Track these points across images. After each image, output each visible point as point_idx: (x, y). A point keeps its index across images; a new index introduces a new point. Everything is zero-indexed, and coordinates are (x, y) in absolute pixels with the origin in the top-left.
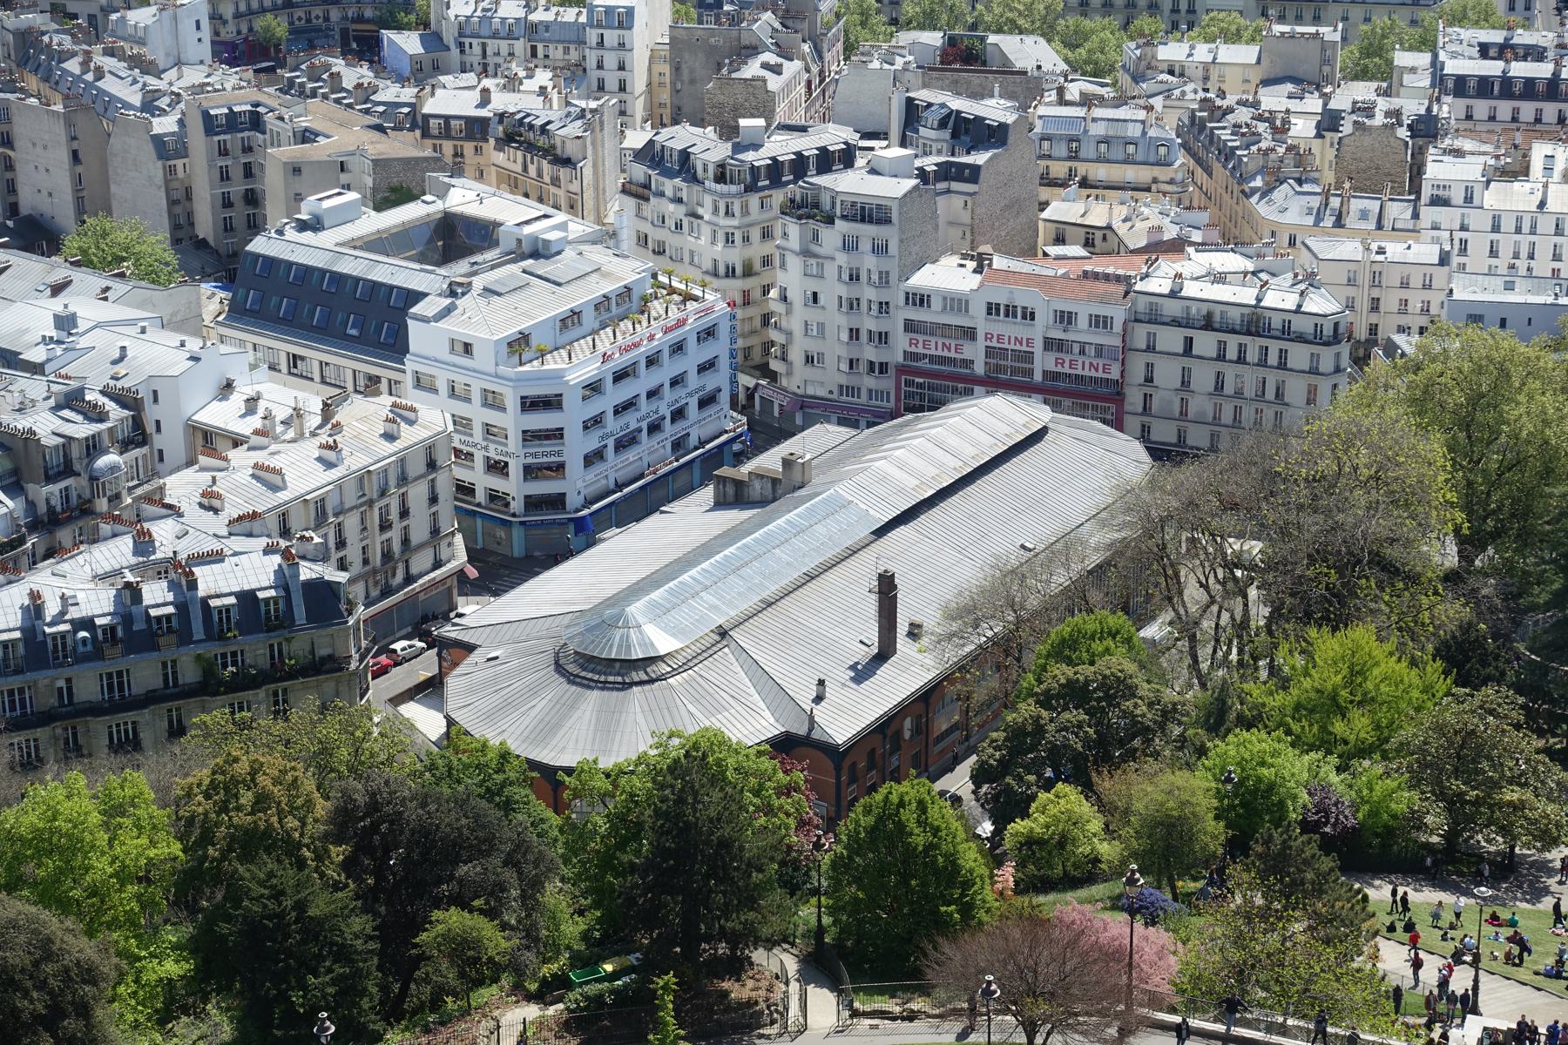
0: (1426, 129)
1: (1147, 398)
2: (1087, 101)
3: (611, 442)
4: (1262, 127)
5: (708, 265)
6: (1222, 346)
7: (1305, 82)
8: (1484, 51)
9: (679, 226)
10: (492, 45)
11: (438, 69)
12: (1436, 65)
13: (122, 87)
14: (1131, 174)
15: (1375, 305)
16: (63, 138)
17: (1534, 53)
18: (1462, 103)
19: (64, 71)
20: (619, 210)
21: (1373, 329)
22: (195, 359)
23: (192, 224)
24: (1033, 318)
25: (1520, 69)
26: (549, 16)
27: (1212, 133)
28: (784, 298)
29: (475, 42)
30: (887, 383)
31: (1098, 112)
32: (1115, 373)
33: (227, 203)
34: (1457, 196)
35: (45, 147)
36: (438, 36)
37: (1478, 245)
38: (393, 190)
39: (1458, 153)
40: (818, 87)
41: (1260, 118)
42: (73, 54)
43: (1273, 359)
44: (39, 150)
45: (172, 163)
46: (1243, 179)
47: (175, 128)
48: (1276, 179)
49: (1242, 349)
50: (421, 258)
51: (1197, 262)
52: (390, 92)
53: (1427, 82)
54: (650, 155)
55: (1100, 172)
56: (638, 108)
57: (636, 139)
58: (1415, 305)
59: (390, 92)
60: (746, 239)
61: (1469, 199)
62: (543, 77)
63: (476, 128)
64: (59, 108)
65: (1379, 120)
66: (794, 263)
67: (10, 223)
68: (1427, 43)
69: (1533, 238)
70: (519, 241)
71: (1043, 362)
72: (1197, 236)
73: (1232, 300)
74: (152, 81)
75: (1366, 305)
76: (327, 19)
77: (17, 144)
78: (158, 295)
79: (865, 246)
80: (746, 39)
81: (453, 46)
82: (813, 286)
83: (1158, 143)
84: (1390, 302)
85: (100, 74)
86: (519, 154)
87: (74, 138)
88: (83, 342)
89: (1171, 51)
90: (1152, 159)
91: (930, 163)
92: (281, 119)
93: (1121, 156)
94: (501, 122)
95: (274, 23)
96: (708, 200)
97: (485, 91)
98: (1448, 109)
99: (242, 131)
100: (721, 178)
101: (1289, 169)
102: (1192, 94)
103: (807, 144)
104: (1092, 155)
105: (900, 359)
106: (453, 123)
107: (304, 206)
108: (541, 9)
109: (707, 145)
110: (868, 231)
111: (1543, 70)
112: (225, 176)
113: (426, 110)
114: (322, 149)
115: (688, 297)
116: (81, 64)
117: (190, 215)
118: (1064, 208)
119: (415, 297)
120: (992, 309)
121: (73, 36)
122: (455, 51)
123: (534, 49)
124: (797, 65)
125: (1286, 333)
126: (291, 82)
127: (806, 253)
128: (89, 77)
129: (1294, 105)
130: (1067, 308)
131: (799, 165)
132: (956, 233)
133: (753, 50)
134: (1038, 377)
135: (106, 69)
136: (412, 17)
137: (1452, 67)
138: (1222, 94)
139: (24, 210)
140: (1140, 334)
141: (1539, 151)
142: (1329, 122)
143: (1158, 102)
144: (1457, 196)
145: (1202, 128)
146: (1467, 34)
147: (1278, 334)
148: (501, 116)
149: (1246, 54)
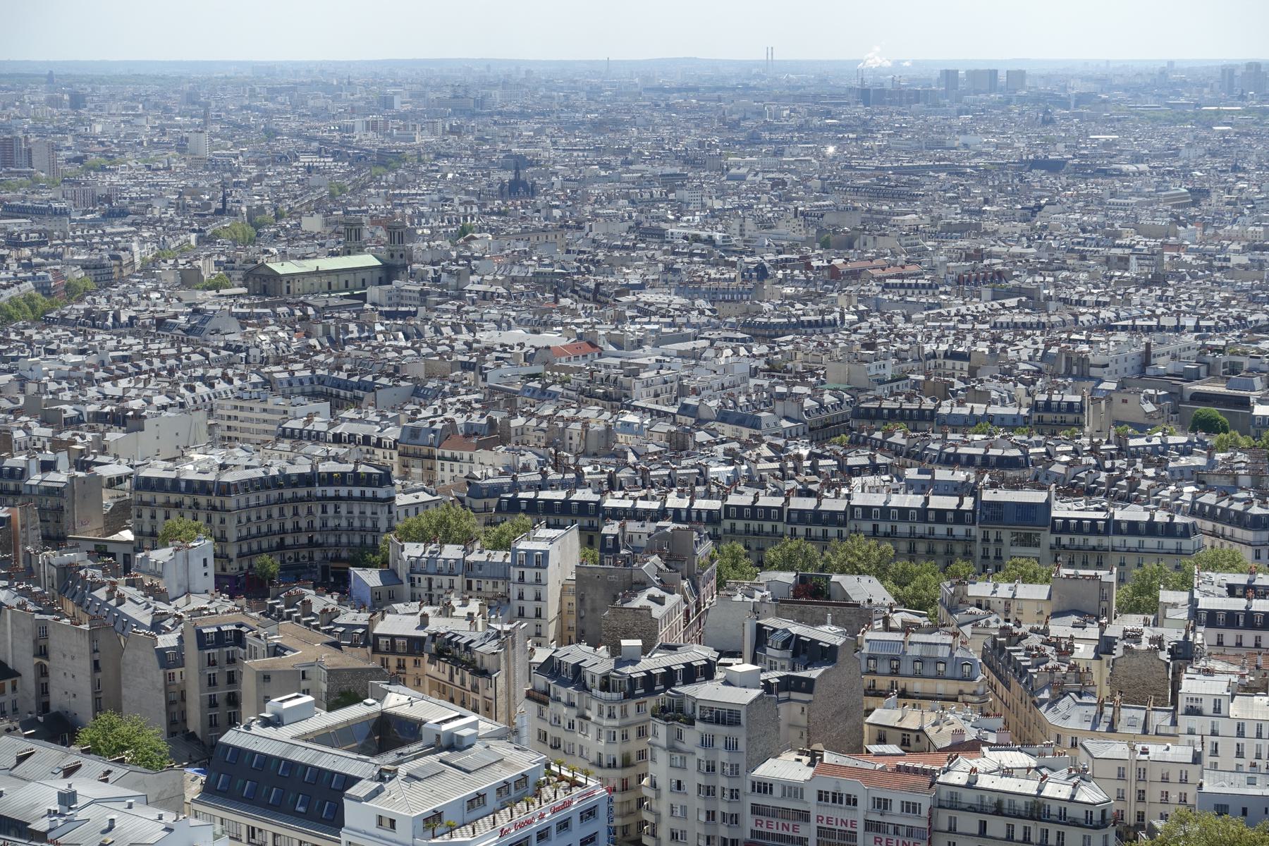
0: (1184, 653)
2: (907, 628)
4: (1049, 650)
5: (594, 758)
6: (1010, 829)
7: (1086, 615)
8: (1232, 590)
9: (571, 725)
10: (436, 580)
11: (393, 598)
12: (1193, 602)
13: (137, 610)
14: (941, 687)
15: (1141, 796)
16: (87, 651)
18: (1213, 633)
19: (94, 597)
20: (526, 712)
21: (1141, 816)
22: (169, 829)
23: (185, 721)
24: (855, 803)
26: (482, 558)
27: (1010, 655)
28: (654, 785)
29: (423, 577)
31: (914, 637)
33: (213, 703)
34: (1208, 707)
35: (73, 658)
36: (394, 573)
37: (1227, 747)
38: (343, 694)
39: (1209, 672)
40: (695, 617)
41: (1048, 643)
42: (103, 585)
44: (68, 660)
45: (171, 671)
46: (1034, 692)
47: (176, 644)
49: (1027, 831)
50: (361, 750)
51: (991, 758)
52: (350, 616)
53: (1185, 615)
54: (551, 668)
55: (917, 685)
56: (551, 631)
57: (541, 656)
58: (1174, 797)
59: (350, 616)
60: (625, 737)
61: (1217, 710)
62: (474, 606)
63: (415, 645)
64: (86, 627)
65: (1145, 645)
66: (662, 757)
67: (41, 719)
68: (1186, 584)
70: (438, 736)
72: (992, 738)
73: (991, 786)
74: (162, 607)
75: (1134, 796)
76: (311, 559)
77: (51, 655)
78: (150, 777)
79: (720, 743)
80: (637, 577)
81: (405, 580)
82: (678, 775)
83: (961, 663)
84: (1154, 793)
85: (121, 600)
86: (447, 666)
87: (96, 651)
88: (81, 815)
89: (979, 589)
90: (958, 675)
91: (774, 676)
92: (258, 636)
93: (933, 673)
94: (433, 641)
95: (269, 562)
97: (425, 617)
99: (227, 646)
100: (605, 687)
101: (1071, 684)
103: (676, 661)
104: (910, 671)
106: (397, 641)
107: (268, 706)
108: (476, 552)
109: (597, 661)
110: (721, 731)
112: (212, 682)
113: (376, 631)
114: (289, 660)
115: (574, 783)
116: (108, 592)
117: (183, 713)
118: (885, 715)
119: (352, 781)
120: (821, 796)
121: (104, 570)
122: (407, 585)
123: (469, 583)
124: (677, 597)
125: (1063, 818)
126: (272, 606)
127: (672, 748)
128: (113, 603)
129: (1077, 633)
130: (883, 795)
131: (669, 677)
132: (795, 734)
133: (643, 585)
135: (127, 596)
136: (379, 558)
137: (1205, 603)
138: (1018, 624)
139: (54, 708)
140: (943, 819)
142: (1105, 646)
143: (967, 630)
144: (1208, 707)
145: (1002, 650)
146: (1216, 577)
147: (1056, 819)
148: (434, 636)
149: (1039, 592)
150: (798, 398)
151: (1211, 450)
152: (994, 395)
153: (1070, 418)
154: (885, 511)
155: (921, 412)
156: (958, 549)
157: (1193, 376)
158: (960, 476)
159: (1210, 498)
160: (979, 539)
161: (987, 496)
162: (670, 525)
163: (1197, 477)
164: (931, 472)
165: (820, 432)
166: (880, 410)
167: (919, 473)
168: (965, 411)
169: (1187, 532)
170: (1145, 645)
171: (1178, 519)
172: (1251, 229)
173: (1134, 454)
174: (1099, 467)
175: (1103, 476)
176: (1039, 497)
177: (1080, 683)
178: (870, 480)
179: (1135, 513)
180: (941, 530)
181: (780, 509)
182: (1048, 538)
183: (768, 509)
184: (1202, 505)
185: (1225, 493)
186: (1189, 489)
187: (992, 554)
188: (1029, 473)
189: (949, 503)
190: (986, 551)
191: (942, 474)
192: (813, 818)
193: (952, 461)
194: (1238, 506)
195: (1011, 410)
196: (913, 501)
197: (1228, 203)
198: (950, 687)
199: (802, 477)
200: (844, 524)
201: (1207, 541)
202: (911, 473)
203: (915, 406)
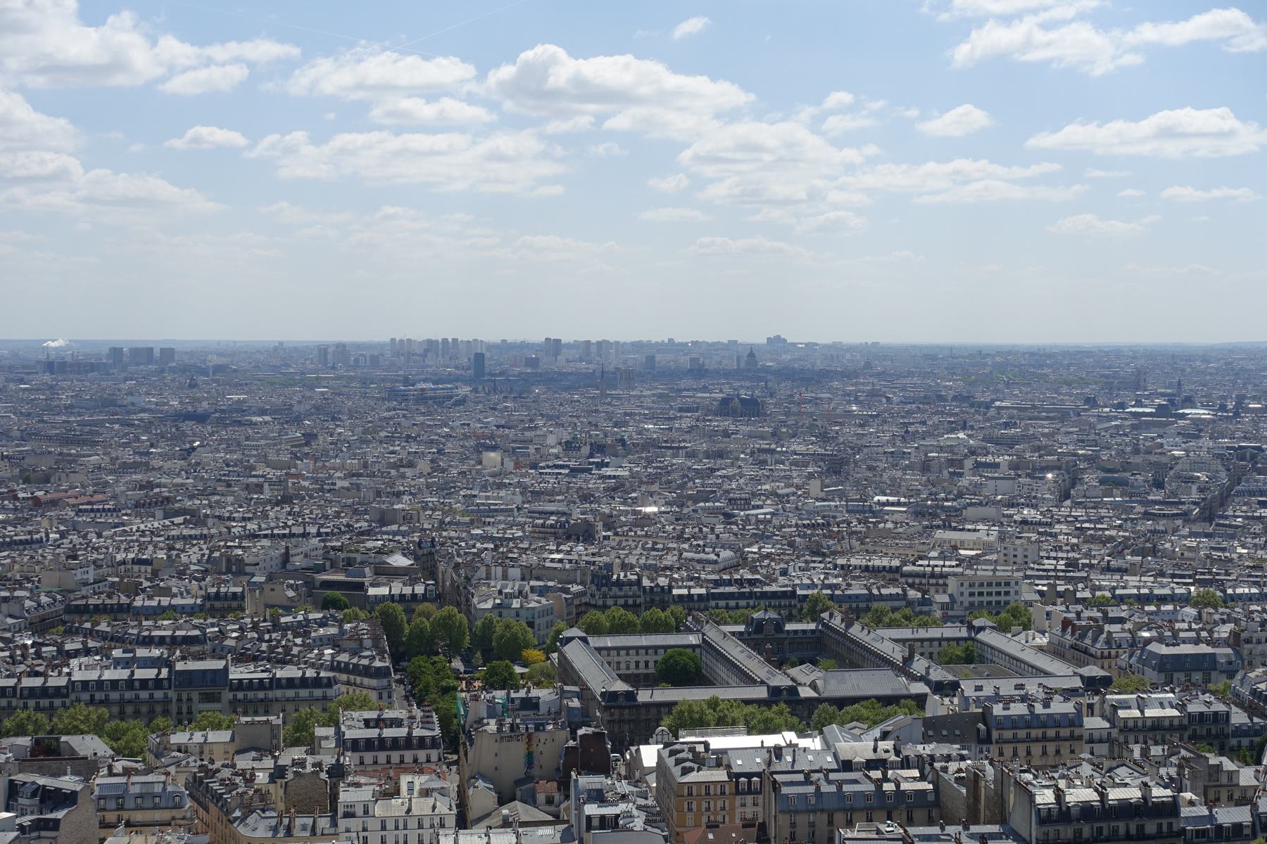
0: (338, 772)
2: (127, 772)
4: (238, 780)
7: (265, 749)
8: (367, 723)
12: (339, 733)
14: (158, 815)
17: (397, 723)
18: (357, 755)
25: (389, 733)
27: (207, 786)
31: (135, 779)
34: (359, 810)
39: (358, 785)
41: (236, 774)
46: (228, 813)
48: (248, 810)
53: (333, 745)
55: (138, 816)
61: (366, 812)
65: (309, 769)
69: (405, 832)
83: (174, 795)
89: (179, 738)
90: (171, 805)
91: (26, 820)
93: (151, 805)
98: (348, 759)
102: (193, 763)
104: (133, 806)
111: (402, 732)
129: (256, 764)
137: (350, 734)
138: (212, 761)
141: (405, 780)
142: (278, 773)
143: (172, 769)
144: (359, 810)
145: (201, 782)
146: (355, 715)
149: (224, 736)
150: (20, 600)
151: (340, 623)
152: (175, 590)
153: (234, 604)
154: (100, 684)
155: (120, 605)
156: (159, 709)
157: (320, 569)
158: (156, 652)
159: (344, 657)
160: (174, 700)
161: (180, 666)
163: (333, 642)
164: (133, 651)
165: (40, 626)
166: (87, 605)
167: (124, 652)
168: (154, 603)
169: (330, 683)
170: (309, 769)
171: (323, 674)
172: (349, 461)
173: (287, 628)
174: (261, 639)
175: (264, 646)
176: (218, 664)
177: (262, 801)
178: (84, 660)
179: (291, 672)
180: (144, 695)
181: (14, 688)
182: (227, 695)
184: (339, 662)
185: (354, 653)
186: (328, 651)
187: (185, 710)
188: (208, 647)
189: (150, 673)
190: (180, 709)
191: (142, 652)
193: (148, 642)
194: (365, 662)
195: (190, 601)
196: (122, 674)
197: (331, 444)
198: (164, 815)
199: (29, 662)
200: (67, 696)
201: (343, 688)
202: (117, 653)
203: (115, 601)
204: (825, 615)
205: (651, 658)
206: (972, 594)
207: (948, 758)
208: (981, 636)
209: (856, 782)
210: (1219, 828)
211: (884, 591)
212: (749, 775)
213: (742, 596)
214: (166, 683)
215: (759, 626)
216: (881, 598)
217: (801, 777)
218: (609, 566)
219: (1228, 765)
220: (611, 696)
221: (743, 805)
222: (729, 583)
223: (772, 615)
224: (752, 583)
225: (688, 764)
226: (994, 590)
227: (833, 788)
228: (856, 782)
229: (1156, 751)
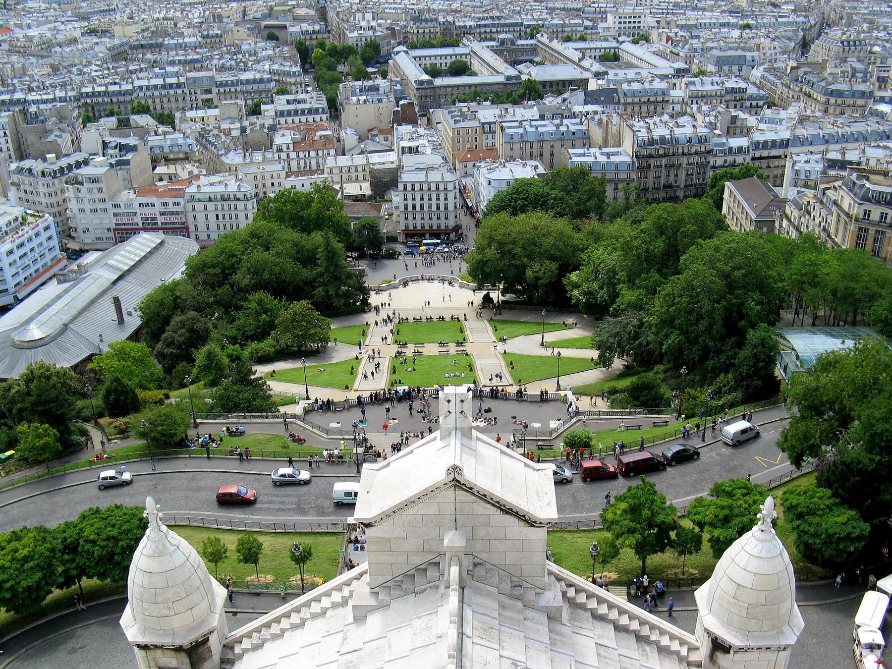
0: (273, 129)
1: (196, 226)
3: (20, 269)
4: (222, 134)
15: (264, 185)
30: (111, 234)
32: (184, 220)
39: (283, 135)
43: (233, 208)
51: (204, 180)
57: (13, 166)
58: (276, 184)
71: (161, 220)
79: (95, 191)
84: (269, 184)
91: (113, 161)
96: (40, 184)
102: (199, 126)
103: (72, 160)
105: (114, 226)
120: (141, 205)
131: (70, 167)
134: (160, 225)
146: (282, 97)
159: (276, 67)
162: (59, 104)
183: (99, 92)
192: (139, 214)
196: (159, 81)
204: (539, 36)
205: (443, 61)
206: (620, 23)
207: (596, 113)
208: (622, 46)
209: (544, 126)
210: (731, 149)
211: (572, 22)
212: (490, 124)
213: (493, 25)
214: (182, 85)
215: (503, 42)
216: (570, 25)
217: (517, 124)
218: (419, 11)
219: (741, 115)
220: (421, 83)
221: (487, 139)
222: (487, 19)
223: (510, 36)
224: (499, 18)
225: (457, 118)
226: (632, 20)
227: (533, 129)
228: (544, 126)
229: (705, 108)
